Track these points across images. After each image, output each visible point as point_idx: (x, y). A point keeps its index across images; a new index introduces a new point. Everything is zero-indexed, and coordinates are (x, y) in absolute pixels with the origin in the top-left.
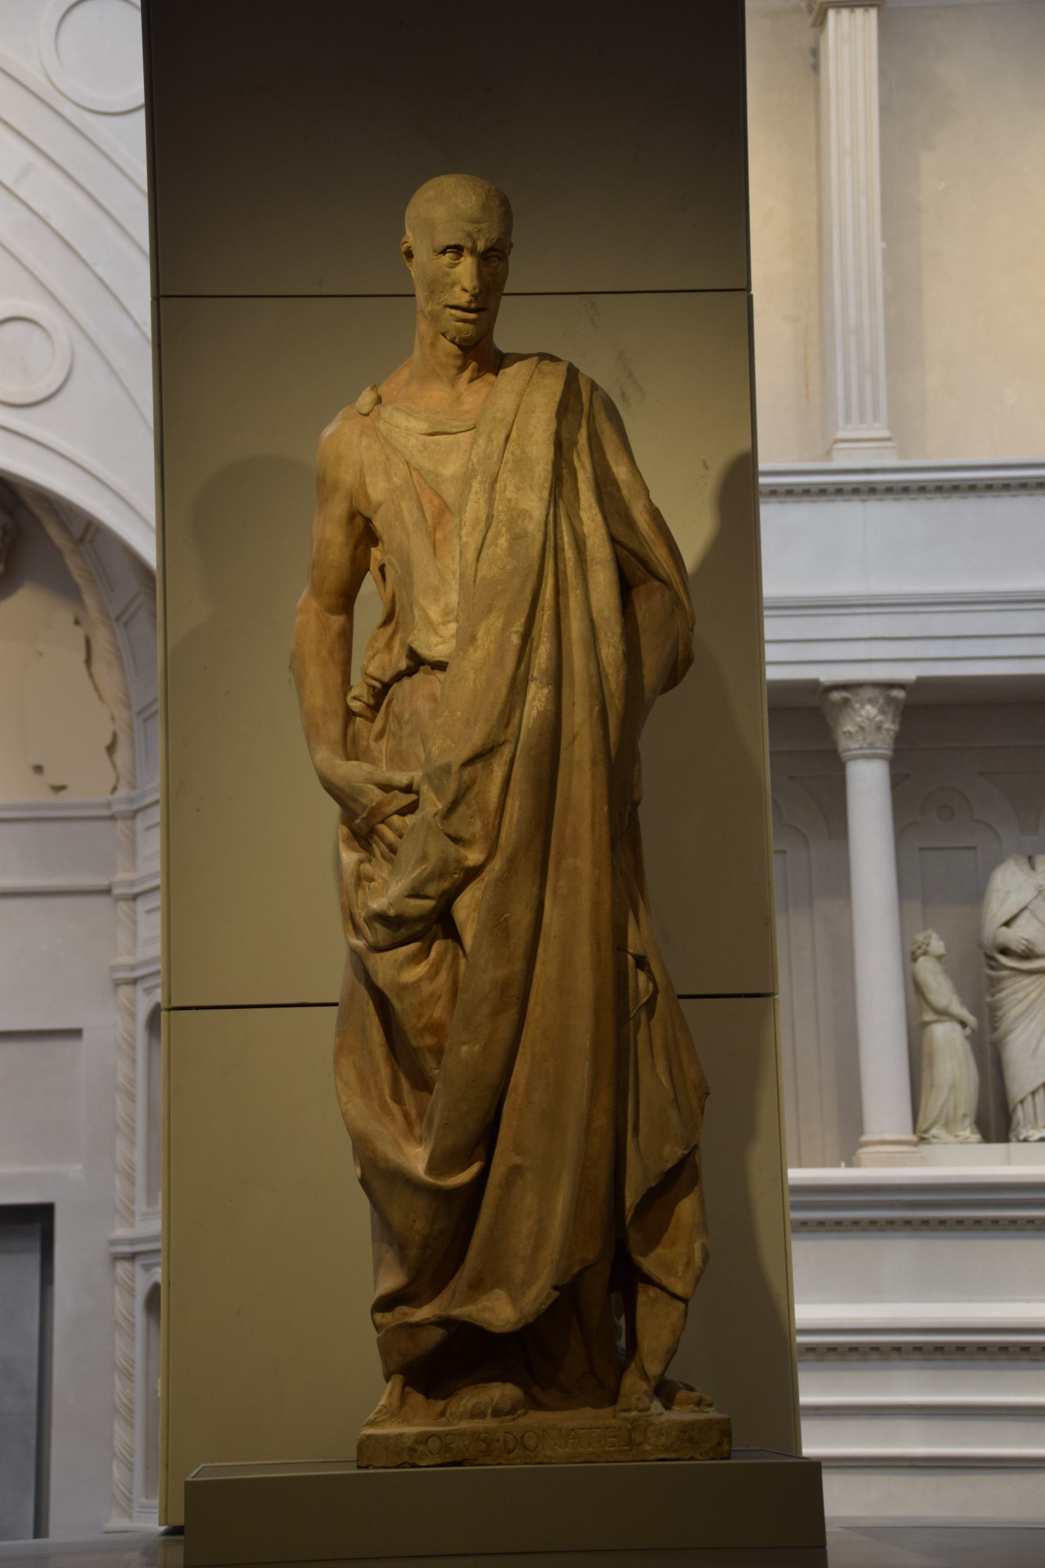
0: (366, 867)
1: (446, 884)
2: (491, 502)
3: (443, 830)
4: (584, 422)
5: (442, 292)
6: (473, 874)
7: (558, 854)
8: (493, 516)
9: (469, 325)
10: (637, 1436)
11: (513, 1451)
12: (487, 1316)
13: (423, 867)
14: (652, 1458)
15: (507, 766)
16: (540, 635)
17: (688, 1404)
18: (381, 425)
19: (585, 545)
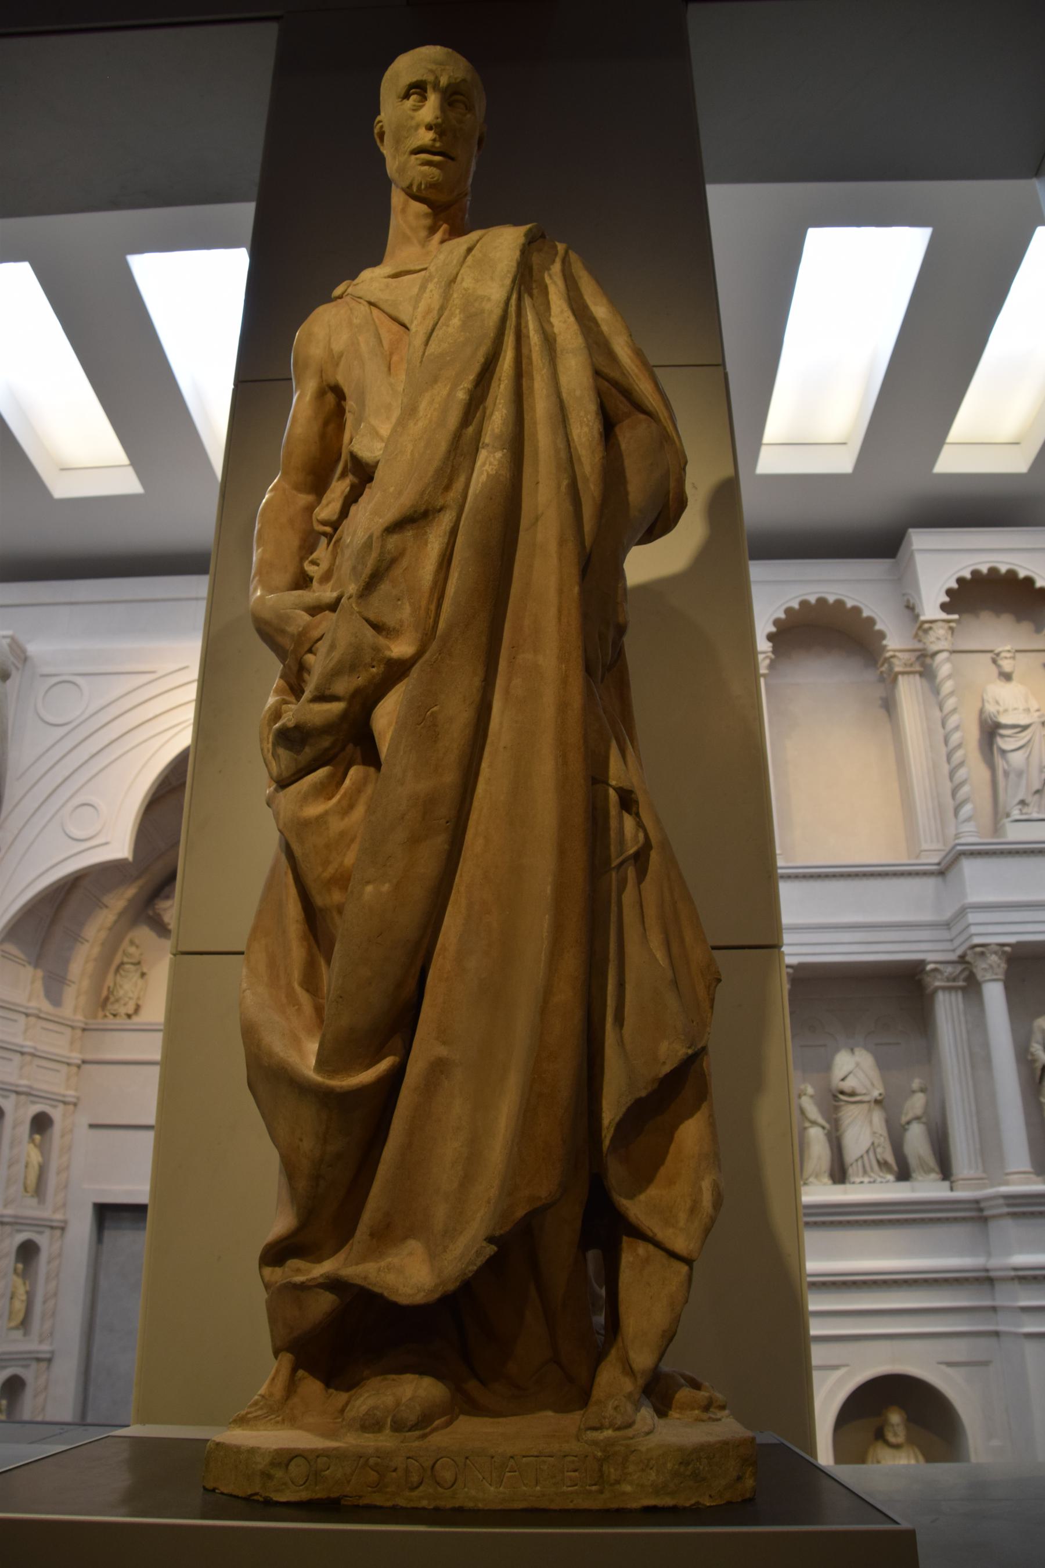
1: (359, 680)
2: (446, 297)
3: (359, 613)
5: (407, 138)
7: (513, 647)
9: (435, 169)
10: (612, 1470)
11: (417, 1487)
12: (390, 1278)
15: (447, 537)
16: (495, 402)
17: (693, 1409)
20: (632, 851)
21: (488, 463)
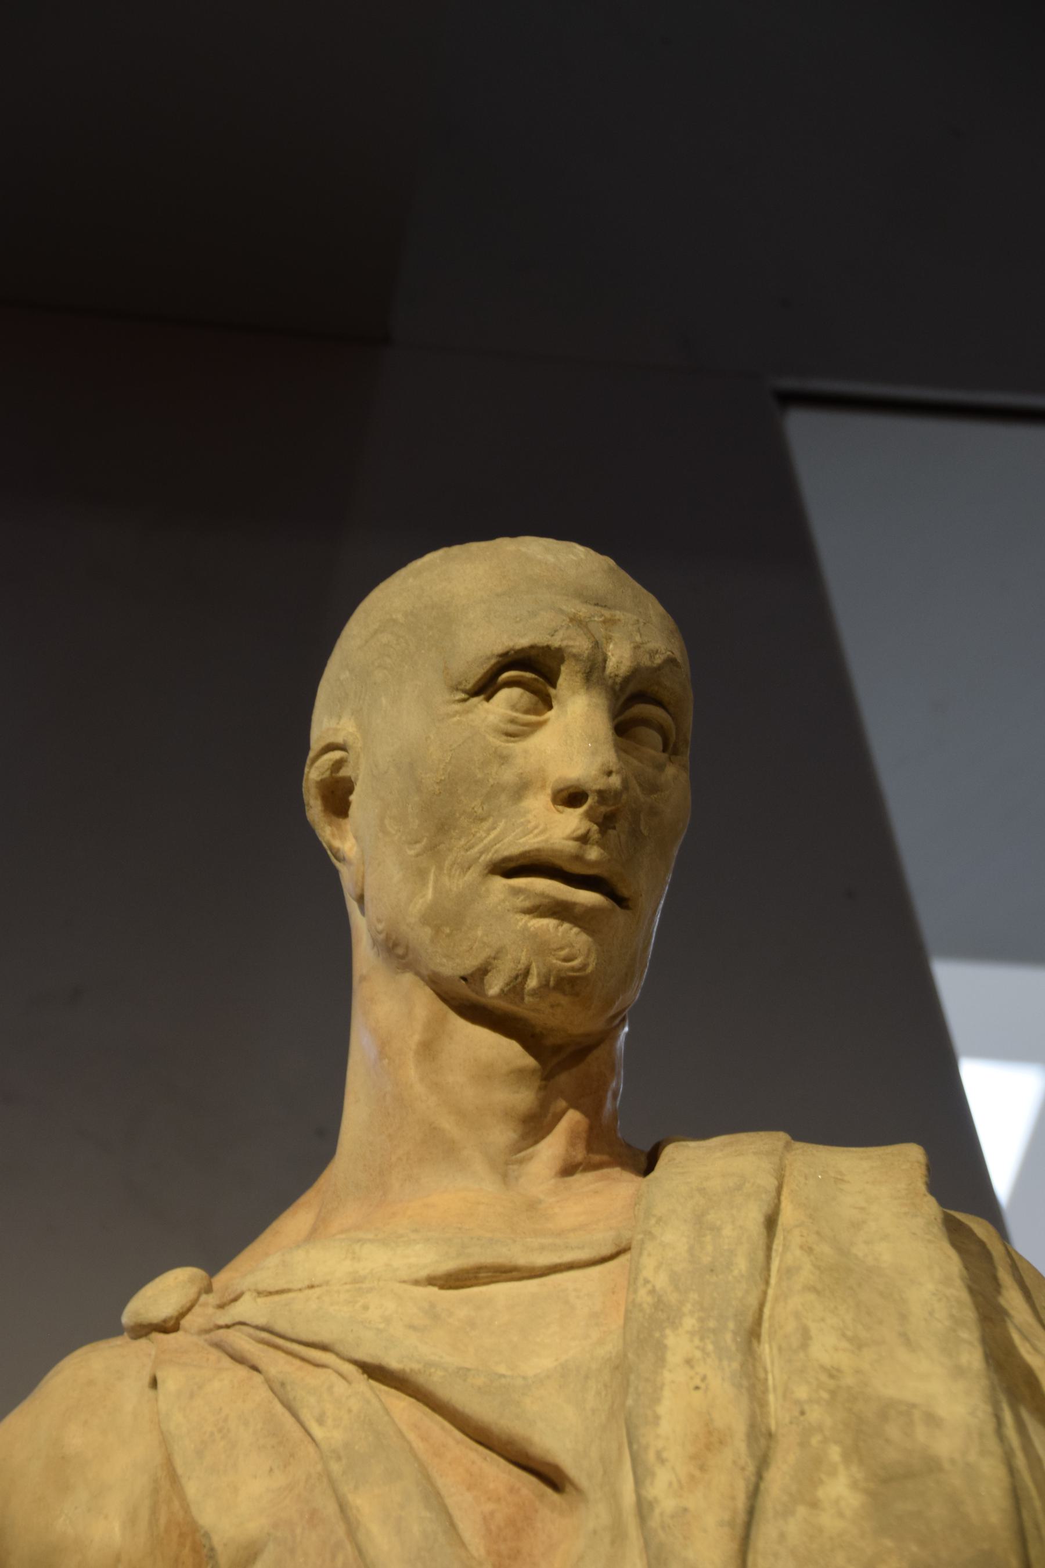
5: (482, 819)
9: (576, 930)
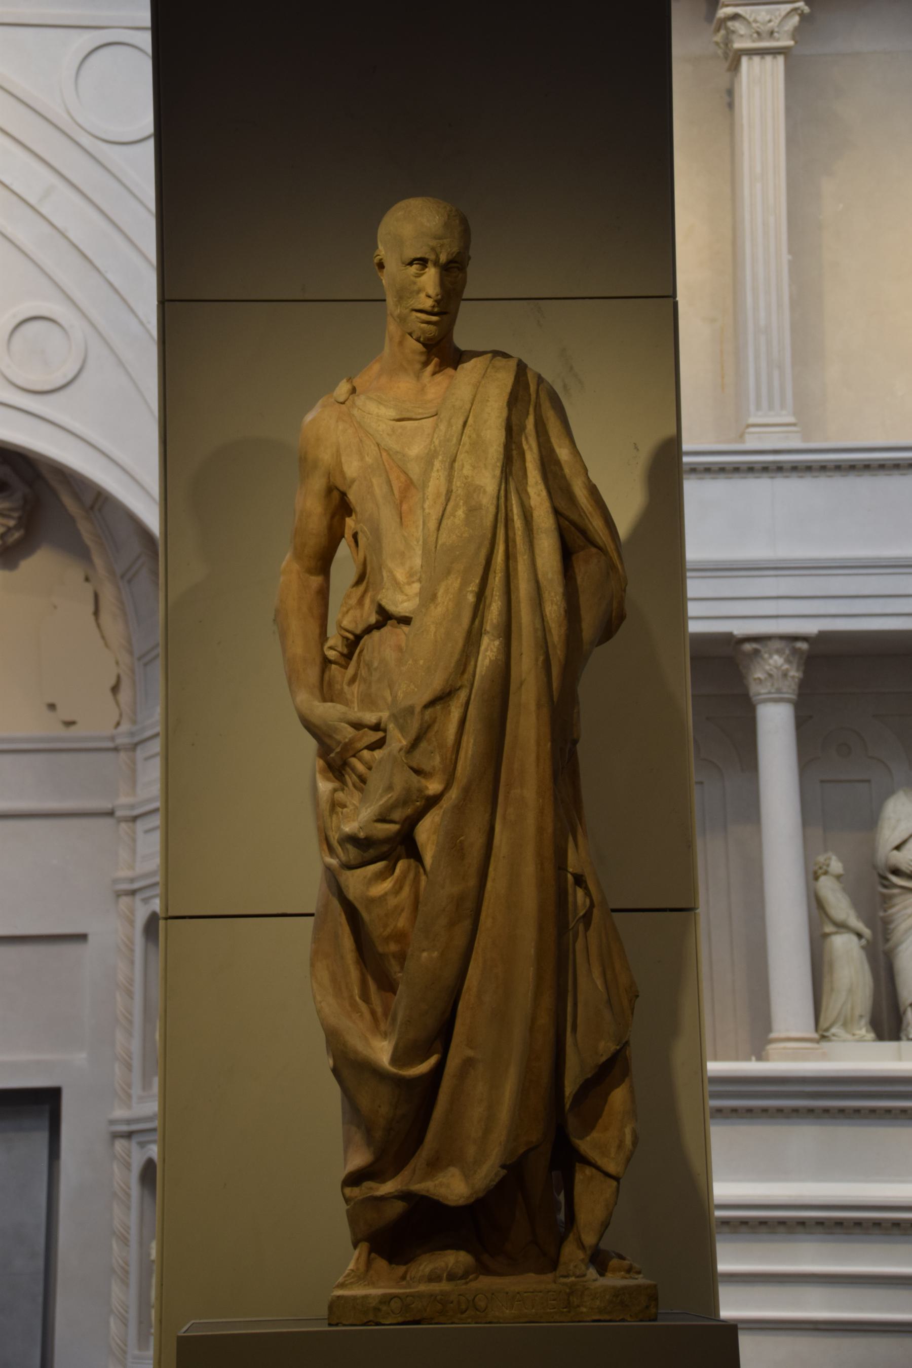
0: (340, 795)
1: (409, 811)
2: (450, 479)
3: (407, 764)
4: (531, 410)
5: (409, 298)
6: (433, 801)
7: (507, 785)
8: (452, 491)
9: (432, 326)
10: (575, 1299)
12: (443, 1191)
13: (390, 795)
14: (588, 1319)
15: (463, 708)
16: (492, 594)
18: (355, 412)
19: (532, 516)
20: (581, 914)
21: (489, 649)
